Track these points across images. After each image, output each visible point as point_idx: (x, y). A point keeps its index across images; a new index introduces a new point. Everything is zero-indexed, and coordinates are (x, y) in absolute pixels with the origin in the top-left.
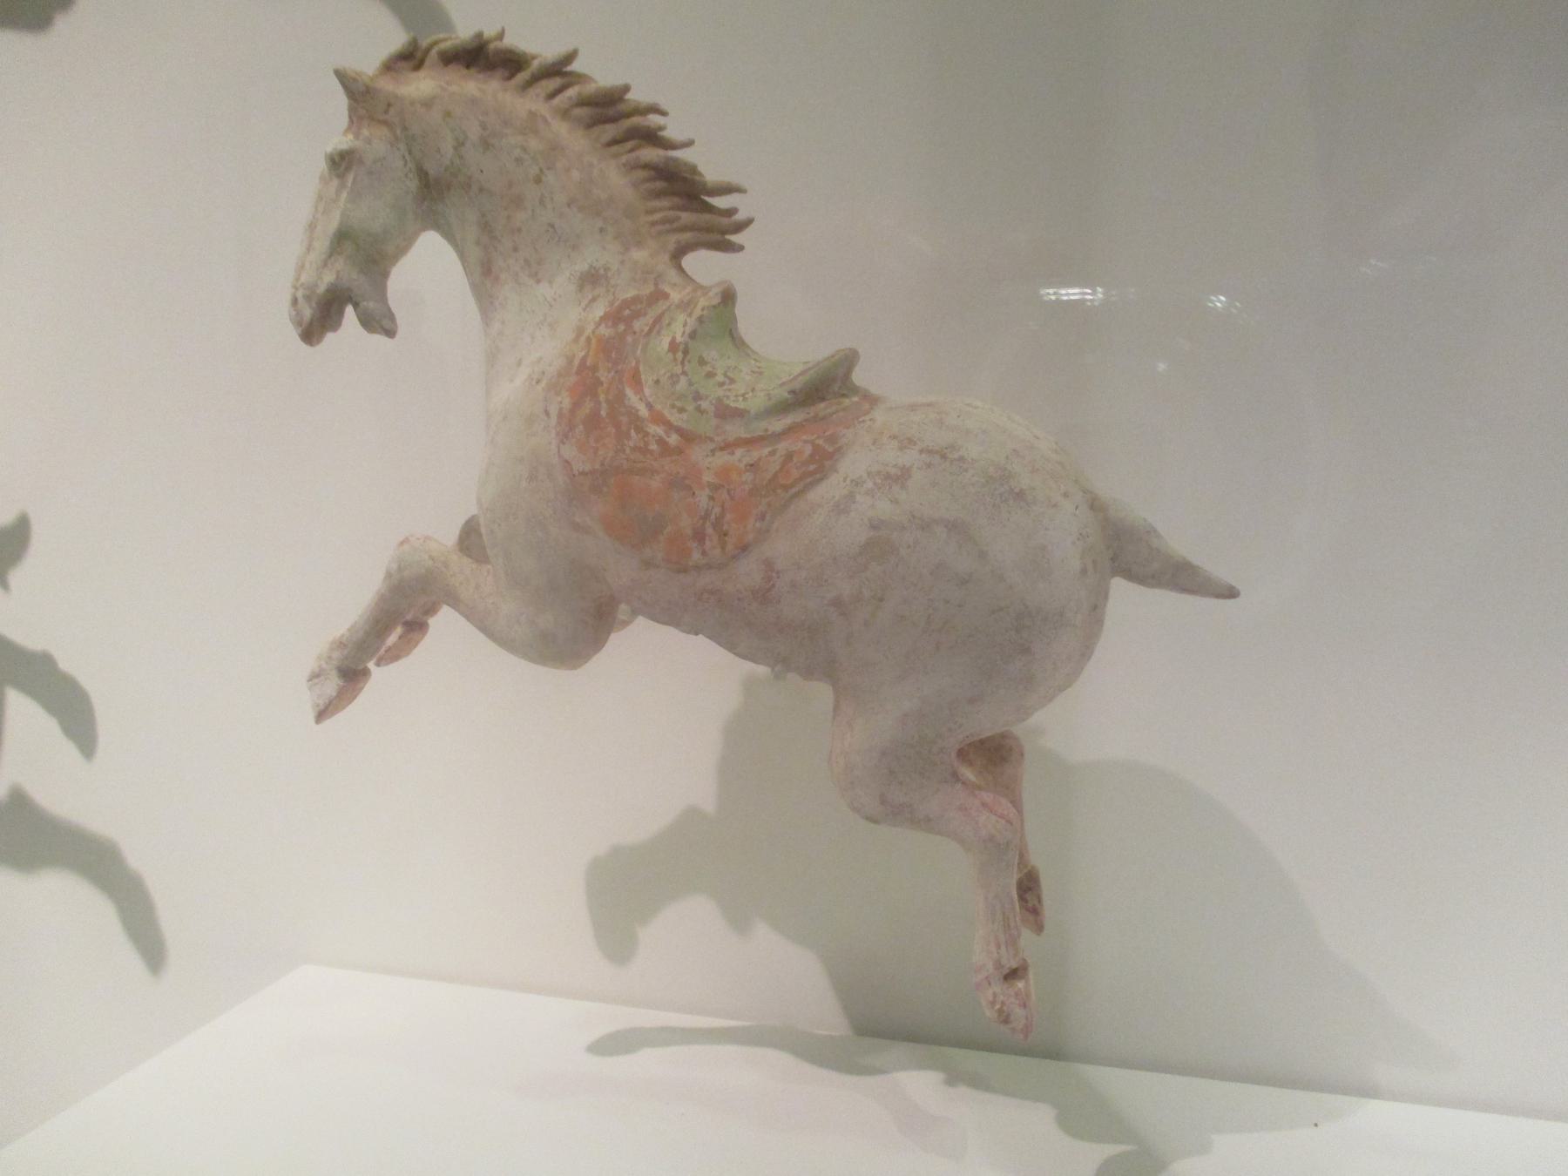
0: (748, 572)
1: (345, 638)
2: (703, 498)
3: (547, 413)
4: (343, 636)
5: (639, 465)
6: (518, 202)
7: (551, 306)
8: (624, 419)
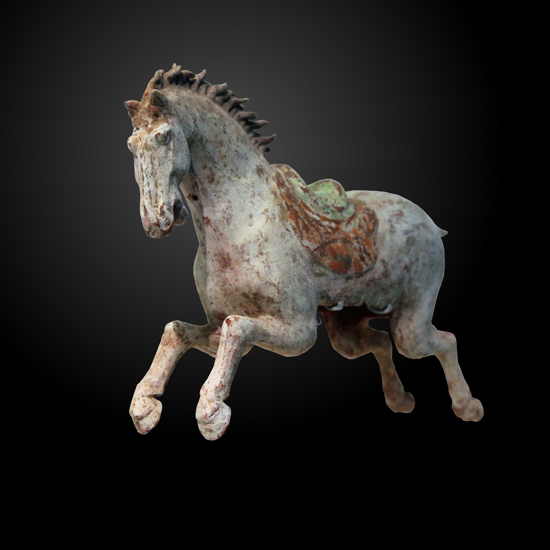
0: (379, 267)
1: (223, 382)
2: (356, 244)
3: (287, 230)
4: (221, 382)
5: (330, 239)
6: (221, 143)
7: (254, 187)
8: (314, 223)
